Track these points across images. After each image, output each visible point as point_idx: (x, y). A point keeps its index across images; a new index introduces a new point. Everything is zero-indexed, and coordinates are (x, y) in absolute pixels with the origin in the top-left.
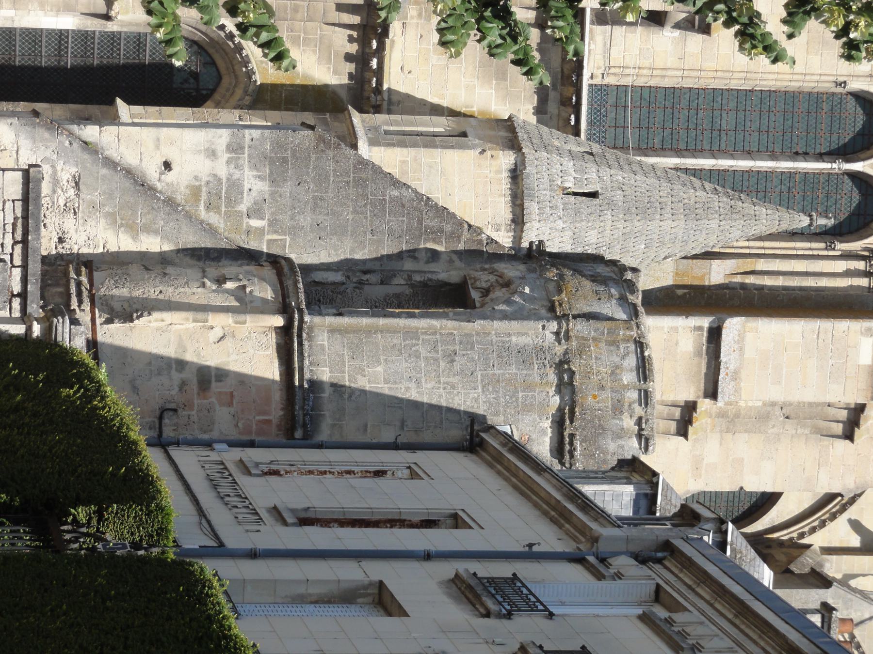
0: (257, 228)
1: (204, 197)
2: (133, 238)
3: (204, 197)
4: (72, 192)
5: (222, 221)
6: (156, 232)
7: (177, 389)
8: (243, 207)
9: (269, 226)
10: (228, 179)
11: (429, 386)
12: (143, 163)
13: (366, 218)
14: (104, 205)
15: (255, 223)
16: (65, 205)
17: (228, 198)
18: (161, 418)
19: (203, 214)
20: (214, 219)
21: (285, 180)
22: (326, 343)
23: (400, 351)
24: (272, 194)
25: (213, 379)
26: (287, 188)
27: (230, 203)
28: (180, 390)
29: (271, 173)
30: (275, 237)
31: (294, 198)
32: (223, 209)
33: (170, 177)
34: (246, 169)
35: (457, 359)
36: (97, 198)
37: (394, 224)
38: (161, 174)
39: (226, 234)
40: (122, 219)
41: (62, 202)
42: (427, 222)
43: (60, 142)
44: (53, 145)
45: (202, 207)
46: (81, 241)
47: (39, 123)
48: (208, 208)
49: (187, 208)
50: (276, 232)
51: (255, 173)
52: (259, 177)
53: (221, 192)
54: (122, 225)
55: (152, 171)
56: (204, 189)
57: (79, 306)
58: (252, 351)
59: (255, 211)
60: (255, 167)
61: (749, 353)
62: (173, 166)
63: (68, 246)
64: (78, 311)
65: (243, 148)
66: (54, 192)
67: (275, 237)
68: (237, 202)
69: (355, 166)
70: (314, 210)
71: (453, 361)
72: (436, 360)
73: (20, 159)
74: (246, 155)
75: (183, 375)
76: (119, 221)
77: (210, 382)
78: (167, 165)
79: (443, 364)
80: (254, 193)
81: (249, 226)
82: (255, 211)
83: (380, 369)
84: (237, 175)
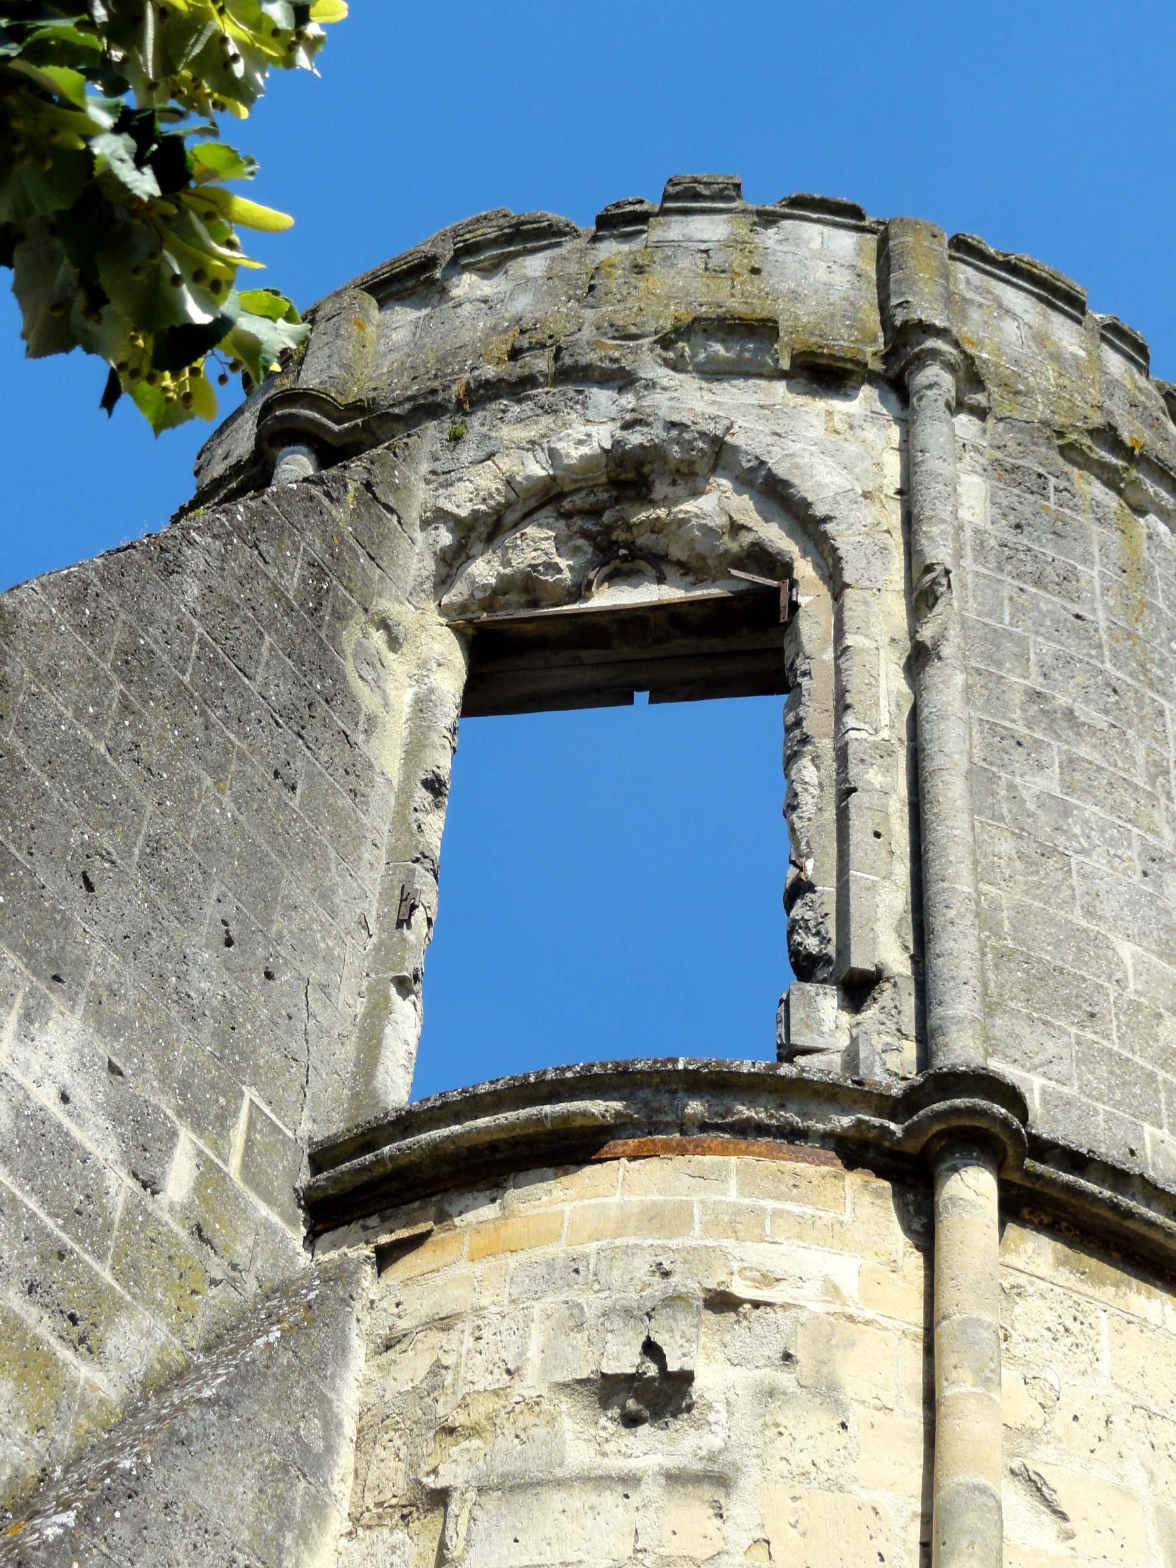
0: (199, 1187)
5: (146, 1319)
8: (119, 1186)
9: (198, 1127)
13: (242, 757)
15: (179, 1178)
19: (101, 1382)
20: (139, 1341)
21: (66, 923)
23: (1047, 852)
24: (101, 1019)
29: (28, 953)
30: (238, 1135)
31: (130, 944)
35: (1062, 700)
37: (281, 692)
39: (195, 1335)
45: (82, 1371)
49: (66, 1442)
50: (224, 1119)
52: (27, 1017)
67: (238, 1135)
69: (80, 628)
70: (185, 917)
71: (1069, 714)
80: (80, 1095)
81: (184, 1212)
83: (1126, 950)
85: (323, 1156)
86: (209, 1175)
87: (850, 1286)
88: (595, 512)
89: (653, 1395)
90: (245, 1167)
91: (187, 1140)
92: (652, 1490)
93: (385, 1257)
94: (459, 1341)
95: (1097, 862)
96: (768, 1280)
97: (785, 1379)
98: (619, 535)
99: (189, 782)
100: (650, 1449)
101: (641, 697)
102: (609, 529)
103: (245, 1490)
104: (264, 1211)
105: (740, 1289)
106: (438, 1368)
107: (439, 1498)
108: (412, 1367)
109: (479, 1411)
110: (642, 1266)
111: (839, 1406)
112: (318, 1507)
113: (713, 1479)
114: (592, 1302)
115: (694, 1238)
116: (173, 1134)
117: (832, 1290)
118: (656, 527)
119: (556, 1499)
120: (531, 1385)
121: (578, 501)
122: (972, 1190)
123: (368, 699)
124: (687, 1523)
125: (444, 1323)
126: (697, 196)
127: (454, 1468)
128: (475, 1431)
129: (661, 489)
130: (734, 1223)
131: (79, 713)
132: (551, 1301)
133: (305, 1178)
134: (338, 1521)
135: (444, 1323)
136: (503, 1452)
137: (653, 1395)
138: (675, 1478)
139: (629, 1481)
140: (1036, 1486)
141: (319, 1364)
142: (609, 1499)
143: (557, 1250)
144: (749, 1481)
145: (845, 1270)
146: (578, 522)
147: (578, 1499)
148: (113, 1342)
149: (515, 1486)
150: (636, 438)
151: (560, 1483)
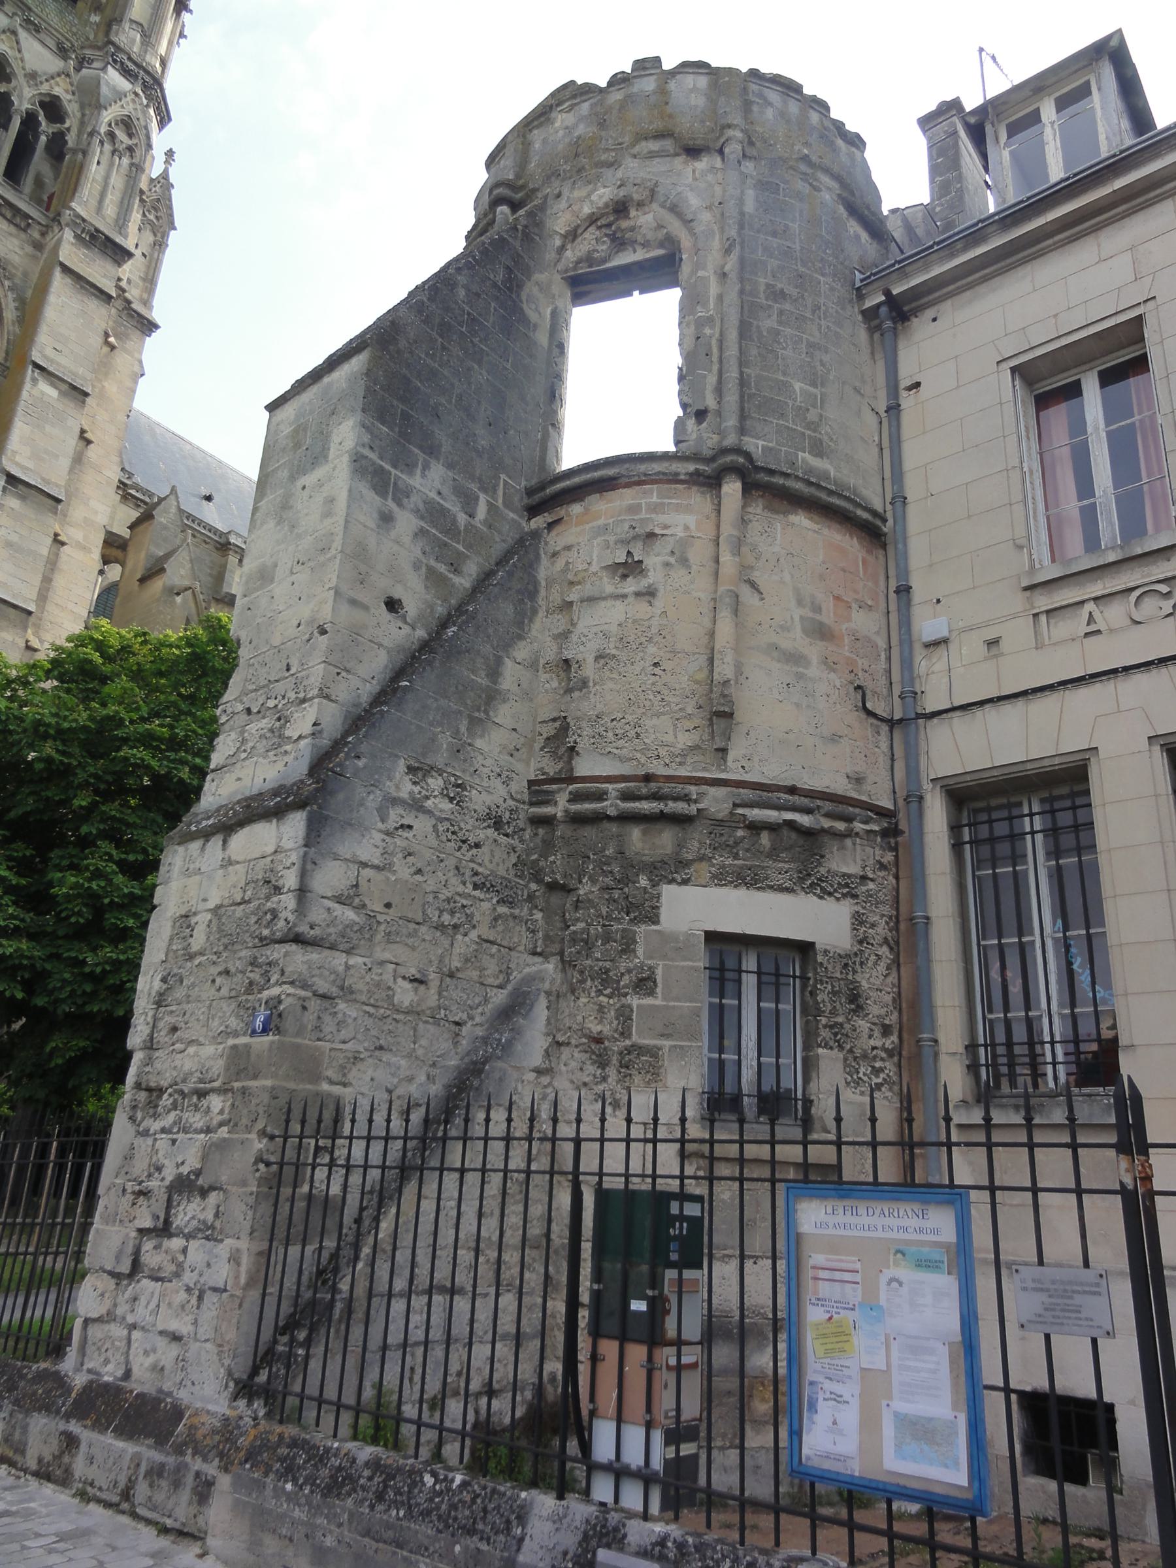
0: (489, 511)
1: (442, 568)
2: (504, 701)
3: (442, 568)
4: (436, 783)
6: (499, 661)
7: (832, 676)
8: (462, 518)
10: (422, 518)
11: (817, 333)
12: (386, 643)
14: (458, 731)
15: (481, 511)
16: (451, 800)
17: (447, 532)
18: (870, 714)
22: (760, 443)
25: (818, 617)
26: (442, 437)
27: (452, 530)
28: (834, 671)
30: (500, 493)
32: (460, 548)
33: (411, 607)
34: (411, 482)
35: (779, 286)
36: (445, 740)
38: (404, 619)
40: (479, 710)
41: (446, 806)
42: (499, 278)
43: (355, 775)
44: (360, 792)
45: (457, 580)
46: (502, 791)
47: (320, 807)
48: (457, 571)
50: (495, 489)
51: (419, 472)
52: (424, 469)
53: (438, 539)
54: (486, 712)
55: (396, 635)
56: (432, 563)
57: (696, 802)
58: (776, 549)
59: (469, 503)
60: (410, 467)
61: (30, 464)
62: (396, 596)
63: (507, 815)
64: (701, 806)
65: (382, 469)
66: (429, 812)
67: (500, 493)
68: (454, 521)
71: (782, 291)
72: (781, 312)
73: (376, 862)
74: (393, 471)
75: (815, 660)
76: (483, 716)
77: (821, 623)
78: (392, 605)
79: (787, 306)
80: (445, 491)
82: (469, 503)
83: (797, 386)
84: (415, 500)
85: (530, 492)
86: (491, 507)
87: (693, 526)
88: (609, 225)
89: (630, 568)
90: (504, 502)
91: (483, 498)
92: (631, 599)
93: (551, 526)
94: (572, 555)
95: (789, 353)
96: (666, 527)
97: (672, 560)
98: (619, 235)
99: (469, 369)
100: (631, 586)
101: (636, 293)
102: (615, 233)
103: (510, 610)
104: (511, 515)
105: (658, 531)
106: (568, 563)
107: (570, 604)
108: (560, 564)
109: (579, 577)
110: (626, 526)
111: (689, 567)
112: (535, 612)
113: (649, 594)
114: (612, 539)
115: (643, 515)
116: (477, 498)
117: (687, 528)
118: (632, 229)
119: (603, 604)
120: (595, 568)
121: (603, 221)
122: (732, 488)
123: (533, 316)
124: (641, 609)
125: (568, 548)
126: (645, 69)
127: (573, 597)
128: (579, 583)
129: (633, 213)
130: (656, 509)
131: (427, 354)
132: (600, 539)
133: (526, 501)
134: (541, 613)
135: (568, 548)
136: (588, 589)
137: (630, 568)
138: (638, 594)
139: (624, 596)
140: (753, 585)
141: (531, 566)
142: (618, 603)
143: (601, 522)
144: (660, 594)
145: (691, 520)
146: (604, 230)
147: (609, 603)
148: (465, 569)
149: (591, 600)
150: (622, 193)
151: (604, 599)
